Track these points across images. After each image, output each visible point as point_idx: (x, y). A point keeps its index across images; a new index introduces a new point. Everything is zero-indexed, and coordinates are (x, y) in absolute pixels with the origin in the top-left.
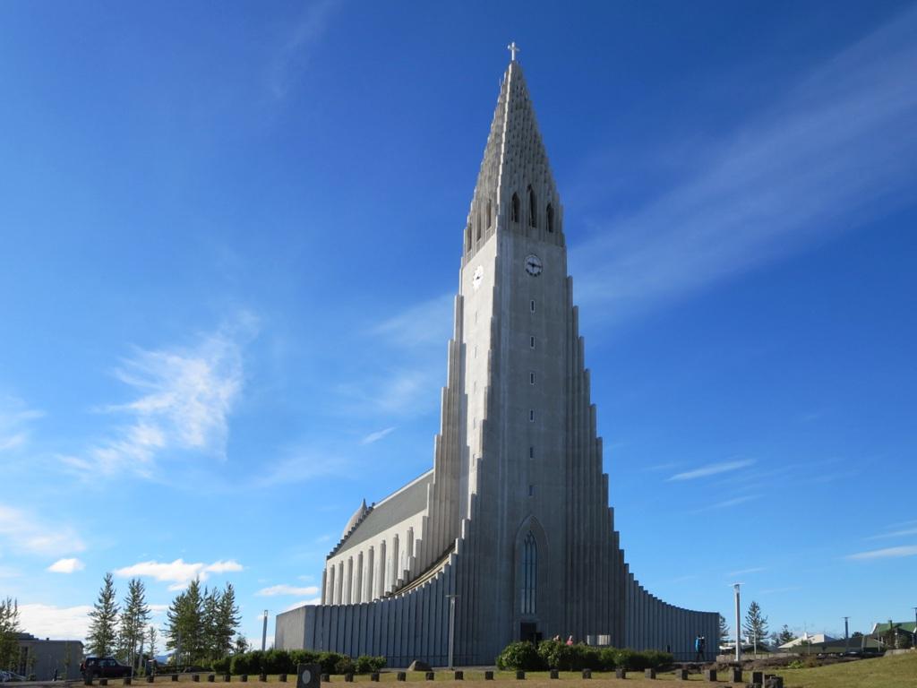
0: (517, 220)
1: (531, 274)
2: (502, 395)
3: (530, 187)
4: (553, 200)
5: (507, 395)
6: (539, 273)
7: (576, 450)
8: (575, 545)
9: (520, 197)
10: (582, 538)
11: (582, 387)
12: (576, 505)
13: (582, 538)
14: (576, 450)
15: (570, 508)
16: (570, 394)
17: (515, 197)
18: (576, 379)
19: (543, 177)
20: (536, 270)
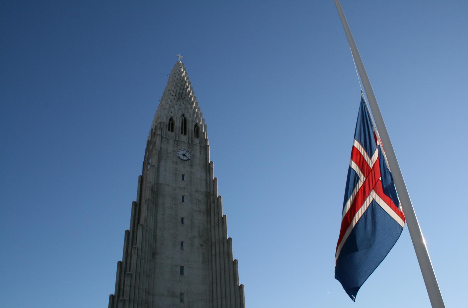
1: (182, 160)
3: (183, 115)
6: (188, 160)
9: (174, 119)
17: (171, 119)
20: (185, 158)
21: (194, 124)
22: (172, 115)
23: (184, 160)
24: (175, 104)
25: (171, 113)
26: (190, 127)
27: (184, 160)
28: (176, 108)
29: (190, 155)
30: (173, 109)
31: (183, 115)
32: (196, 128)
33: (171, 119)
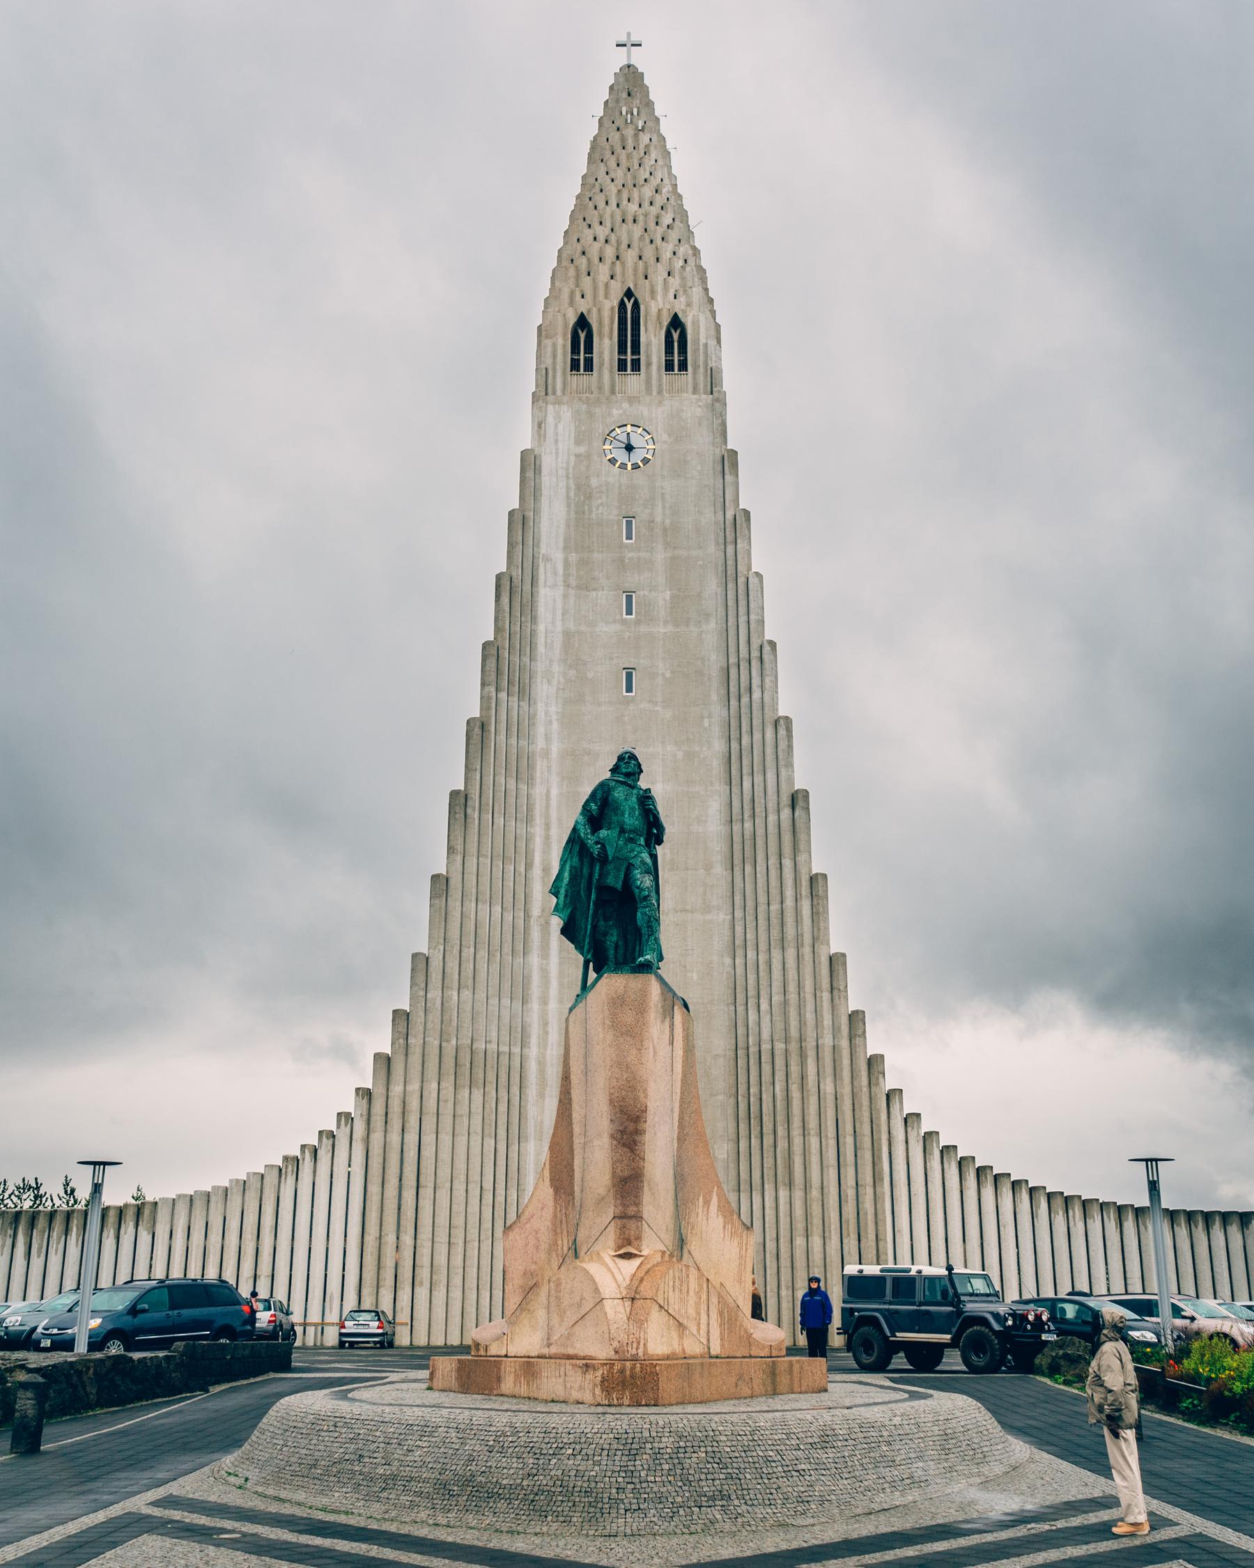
0: (589, 366)
1: (623, 466)
2: (540, 730)
3: (629, 294)
4: (689, 305)
5: (555, 726)
7: (748, 825)
8: (753, 1050)
10: (766, 1035)
11: (756, 682)
12: (751, 954)
13: (766, 1035)
14: (748, 825)
15: (740, 961)
16: (733, 702)
17: (582, 322)
18: (744, 666)
19: (661, 270)
21: (666, 321)
22: (583, 306)
23: (629, 467)
24: (596, 260)
25: (583, 297)
26: (653, 340)
27: (629, 467)
28: (603, 272)
29: (651, 441)
30: (587, 282)
31: (629, 294)
32: (678, 331)
33: (582, 322)
